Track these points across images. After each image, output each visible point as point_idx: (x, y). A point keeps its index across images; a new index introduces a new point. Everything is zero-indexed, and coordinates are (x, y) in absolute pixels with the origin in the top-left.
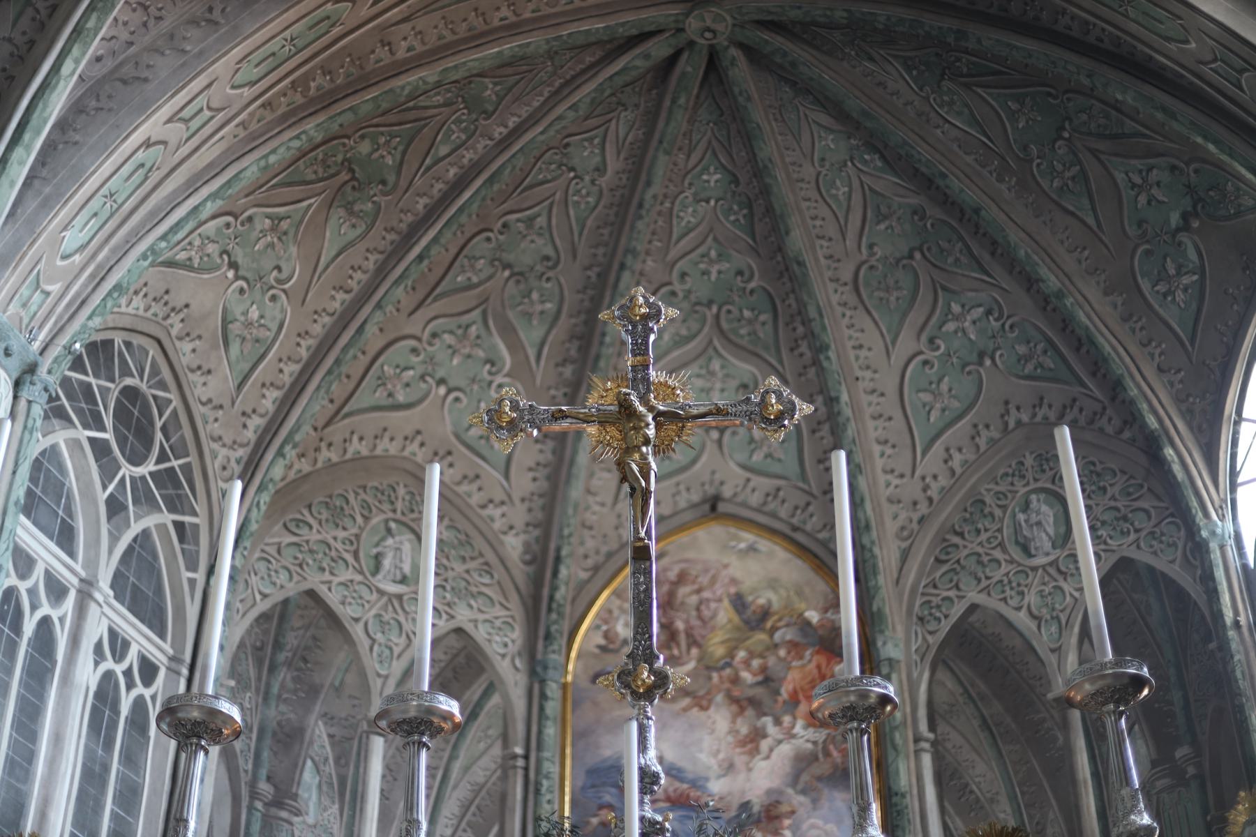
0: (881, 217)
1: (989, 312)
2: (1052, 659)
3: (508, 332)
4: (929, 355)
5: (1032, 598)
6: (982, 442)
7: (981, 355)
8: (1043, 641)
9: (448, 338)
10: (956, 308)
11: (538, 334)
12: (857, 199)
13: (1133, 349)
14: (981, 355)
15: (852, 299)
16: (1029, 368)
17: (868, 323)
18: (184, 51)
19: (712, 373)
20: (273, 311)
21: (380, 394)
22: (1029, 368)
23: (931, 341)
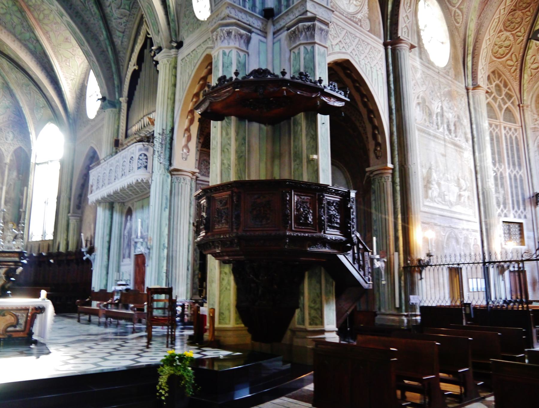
2: (6, 157)
5: (5, 147)
6: (4, 120)
8: (5, 154)
13: (31, 119)
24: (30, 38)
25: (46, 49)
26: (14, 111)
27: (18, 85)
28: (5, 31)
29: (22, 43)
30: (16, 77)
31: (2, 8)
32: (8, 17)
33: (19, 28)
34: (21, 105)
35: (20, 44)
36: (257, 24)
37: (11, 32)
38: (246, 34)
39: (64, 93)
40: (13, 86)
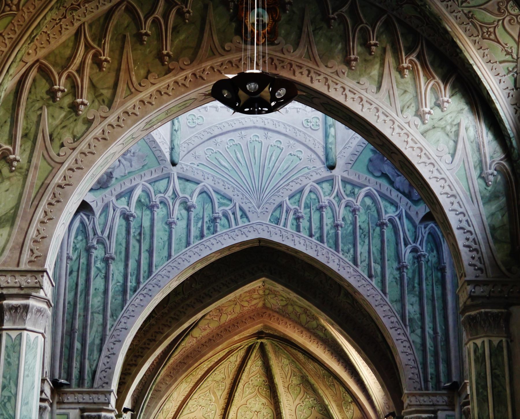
0: (294, 376)
1: (315, 400)
3: (214, 393)
4: (302, 404)
7: (312, 407)
9: (202, 397)
10: (308, 397)
11: (220, 394)
12: (290, 371)
14: (312, 407)
15: (287, 391)
16: (321, 412)
17: (290, 396)
18: (167, 384)
19: (256, 400)
20: (171, 404)
21: (189, 411)
22: (321, 412)
23: (303, 402)
24: (318, 326)
25: (336, 337)
26: (321, 410)
27: (319, 378)
28: (291, 323)
29: (311, 332)
30: (314, 367)
31: (282, 300)
32: (290, 308)
33: (304, 318)
34: (327, 402)
35: (308, 335)
36: (441, 400)
37: (296, 322)
38: (429, 417)
39: (368, 387)
40: (312, 381)
